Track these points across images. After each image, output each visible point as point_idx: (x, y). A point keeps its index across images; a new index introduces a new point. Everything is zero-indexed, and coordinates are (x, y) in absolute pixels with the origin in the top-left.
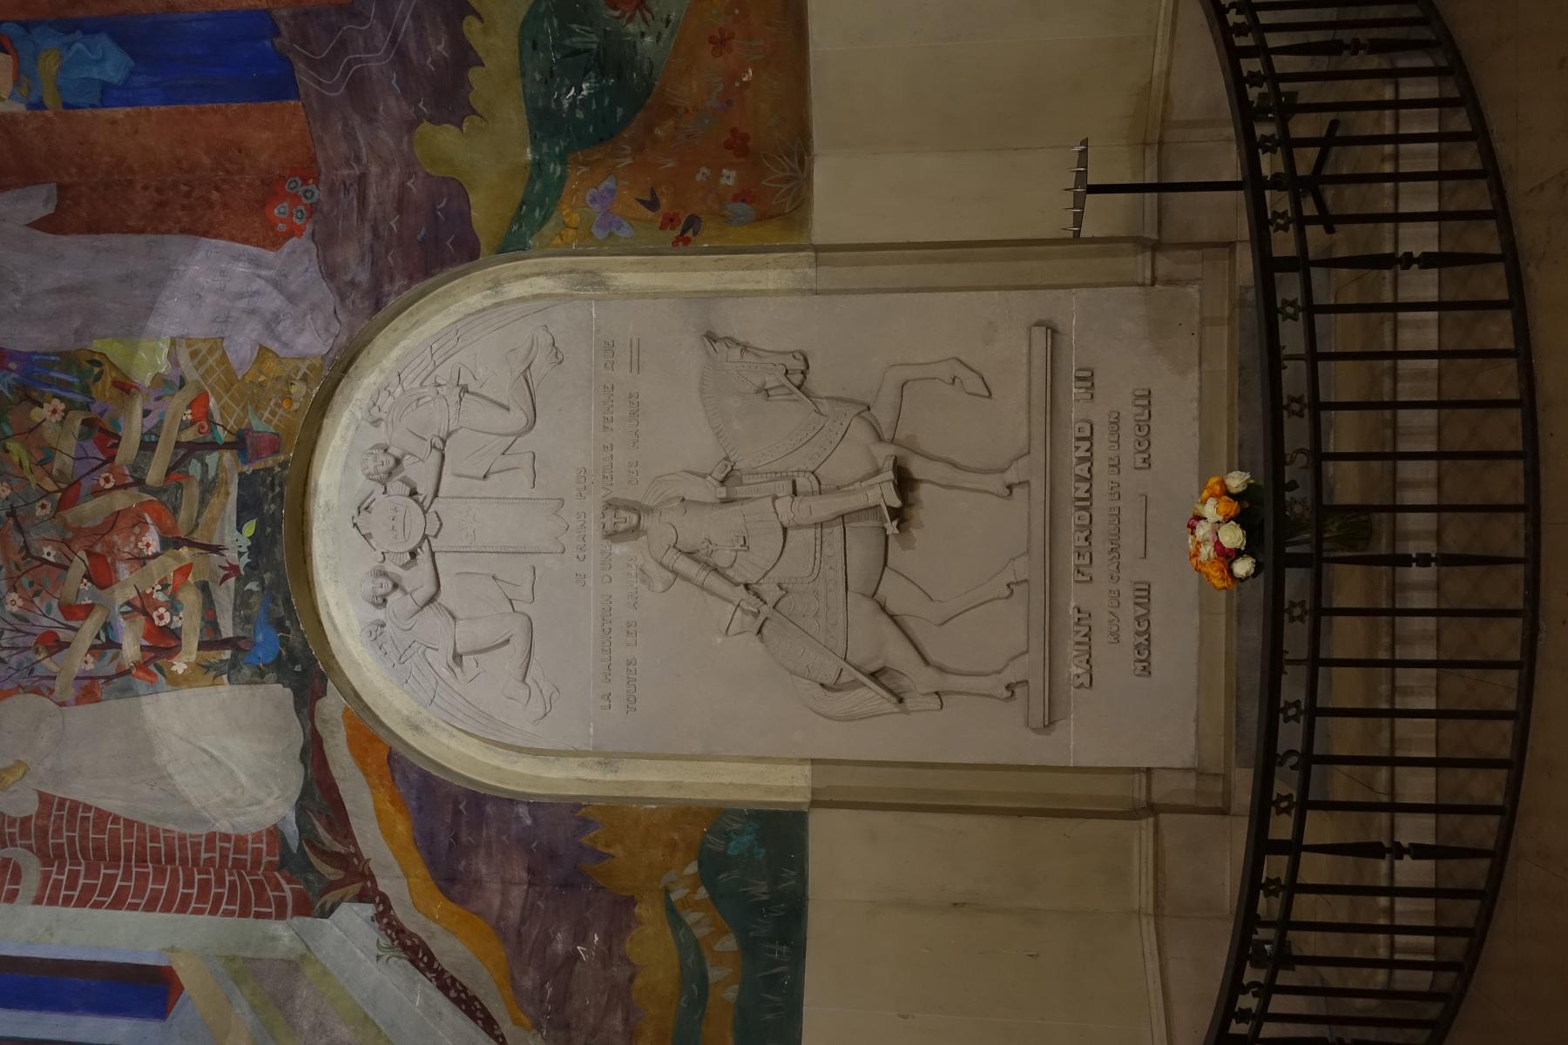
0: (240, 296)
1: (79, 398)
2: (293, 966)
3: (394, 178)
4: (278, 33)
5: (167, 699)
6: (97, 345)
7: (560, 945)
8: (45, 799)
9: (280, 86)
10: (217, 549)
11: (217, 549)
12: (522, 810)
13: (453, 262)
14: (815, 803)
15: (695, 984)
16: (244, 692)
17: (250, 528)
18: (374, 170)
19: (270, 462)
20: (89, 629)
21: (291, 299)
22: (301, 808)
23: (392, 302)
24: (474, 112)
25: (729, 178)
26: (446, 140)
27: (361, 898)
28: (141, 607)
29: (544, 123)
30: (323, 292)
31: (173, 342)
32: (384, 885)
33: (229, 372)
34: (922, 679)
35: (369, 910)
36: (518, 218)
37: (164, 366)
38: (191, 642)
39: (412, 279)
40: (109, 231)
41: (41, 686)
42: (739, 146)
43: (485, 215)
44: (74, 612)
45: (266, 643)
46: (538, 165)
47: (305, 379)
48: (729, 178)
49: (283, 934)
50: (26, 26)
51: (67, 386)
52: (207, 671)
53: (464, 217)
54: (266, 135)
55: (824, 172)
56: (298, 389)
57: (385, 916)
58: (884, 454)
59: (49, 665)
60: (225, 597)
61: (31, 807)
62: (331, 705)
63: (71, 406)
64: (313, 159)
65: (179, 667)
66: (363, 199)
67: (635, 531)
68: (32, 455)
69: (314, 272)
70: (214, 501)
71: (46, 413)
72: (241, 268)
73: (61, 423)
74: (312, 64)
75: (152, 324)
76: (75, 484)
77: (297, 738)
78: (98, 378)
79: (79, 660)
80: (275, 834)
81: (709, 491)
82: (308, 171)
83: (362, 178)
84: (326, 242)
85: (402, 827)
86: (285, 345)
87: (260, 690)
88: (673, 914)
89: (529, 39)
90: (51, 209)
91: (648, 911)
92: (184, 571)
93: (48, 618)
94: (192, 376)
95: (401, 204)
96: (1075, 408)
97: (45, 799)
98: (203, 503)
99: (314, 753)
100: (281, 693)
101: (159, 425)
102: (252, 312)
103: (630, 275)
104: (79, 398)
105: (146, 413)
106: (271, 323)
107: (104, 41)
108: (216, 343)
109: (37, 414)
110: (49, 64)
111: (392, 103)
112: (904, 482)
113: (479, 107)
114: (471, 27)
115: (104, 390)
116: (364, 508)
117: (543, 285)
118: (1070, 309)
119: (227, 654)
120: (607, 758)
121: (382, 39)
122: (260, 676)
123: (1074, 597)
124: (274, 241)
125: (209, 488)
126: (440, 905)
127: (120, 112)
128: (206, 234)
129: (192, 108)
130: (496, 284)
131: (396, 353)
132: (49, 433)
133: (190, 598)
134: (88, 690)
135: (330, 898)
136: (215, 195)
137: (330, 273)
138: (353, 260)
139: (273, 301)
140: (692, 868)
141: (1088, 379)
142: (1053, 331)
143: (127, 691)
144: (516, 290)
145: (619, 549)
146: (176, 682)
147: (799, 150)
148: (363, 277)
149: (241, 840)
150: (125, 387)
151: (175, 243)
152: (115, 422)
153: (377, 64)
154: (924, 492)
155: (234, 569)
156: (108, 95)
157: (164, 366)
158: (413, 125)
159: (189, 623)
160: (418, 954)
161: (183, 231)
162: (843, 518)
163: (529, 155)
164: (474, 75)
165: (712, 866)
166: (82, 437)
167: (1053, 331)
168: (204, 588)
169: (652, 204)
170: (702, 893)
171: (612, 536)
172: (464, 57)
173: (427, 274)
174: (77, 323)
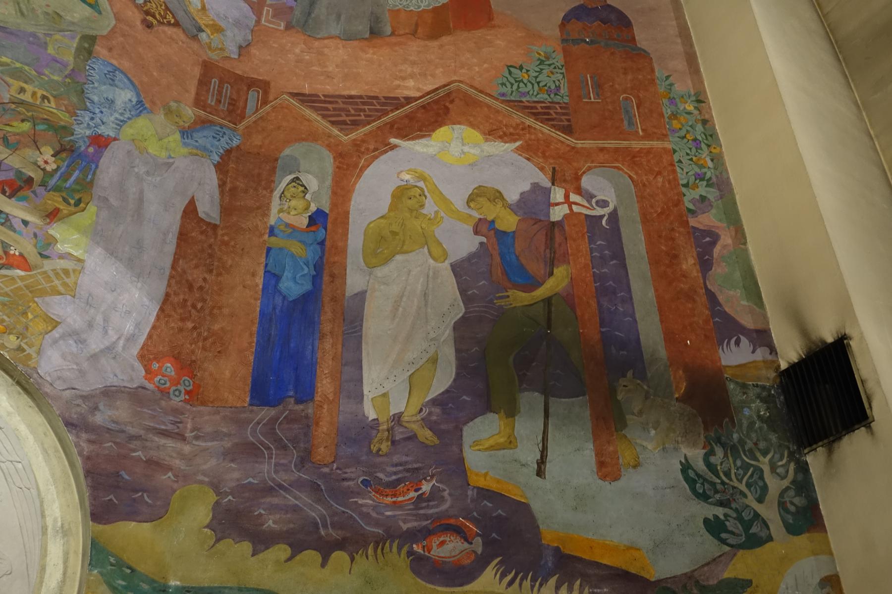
0: (106, 320)
1: (52, 182)
3: (177, 463)
4: (299, 401)
6: (92, 208)
13: (94, 498)
18: (187, 449)
21: (94, 357)
23: (70, 438)
24: (218, 540)
30: (93, 383)
31: (79, 260)
33: (43, 293)
36: (120, 564)
37: (61, 247)
39: (87, 459)
40: (178, 246)
47: (20, 349)
50: (322, 243)
51: (66, 176)
53: (132, 515)
54: (227, 373)
56: (12, 341)
64: (203, 403)
66: (165, 434)
68: (14, 135)
69: (112, 381)
71: (46, 156)
72: (129, 327)
73: (35, 164)
74: (273, 420)
75: (99, 250)
78: (65, 200)
82: (194, 396)
83: (182, 437)
84: (137, 396)
86: (55, 342)
90: (201, 215)
94: (48, 265)
95: (154, 464)
101: (12, 228)
102: (90, 325)
104: (52, 182)
105: (25, 223)
106: (76, 335)
107: (308, 286)
108: (72, 291)
109: (47, 152)
110: (296, 248)
111: (236, 475)
113: (221, 546)
114: (281, 551)
115: (55, 201)
121: (283, 478)
124: (143, 357)
127: (260, 281)
128: (162, 309)
129: (255, 328)
130: (65, 532)
131: (23, 429)
132: (30, 153)
136: (190, 325)
137: (109, 393)
139: (96, 343)
144: (55, 550)
148: (98, 419)
150: (53, 215)
151: (161, 288)
152: (25, 199)
156: (273, 277)
157: (61, 247)
158: (216, 487)
161: (167, 295)
163: (174, 583)
164: (246, 547)
166: (19, 173)
173: (88, 473)
174: (113, 201)
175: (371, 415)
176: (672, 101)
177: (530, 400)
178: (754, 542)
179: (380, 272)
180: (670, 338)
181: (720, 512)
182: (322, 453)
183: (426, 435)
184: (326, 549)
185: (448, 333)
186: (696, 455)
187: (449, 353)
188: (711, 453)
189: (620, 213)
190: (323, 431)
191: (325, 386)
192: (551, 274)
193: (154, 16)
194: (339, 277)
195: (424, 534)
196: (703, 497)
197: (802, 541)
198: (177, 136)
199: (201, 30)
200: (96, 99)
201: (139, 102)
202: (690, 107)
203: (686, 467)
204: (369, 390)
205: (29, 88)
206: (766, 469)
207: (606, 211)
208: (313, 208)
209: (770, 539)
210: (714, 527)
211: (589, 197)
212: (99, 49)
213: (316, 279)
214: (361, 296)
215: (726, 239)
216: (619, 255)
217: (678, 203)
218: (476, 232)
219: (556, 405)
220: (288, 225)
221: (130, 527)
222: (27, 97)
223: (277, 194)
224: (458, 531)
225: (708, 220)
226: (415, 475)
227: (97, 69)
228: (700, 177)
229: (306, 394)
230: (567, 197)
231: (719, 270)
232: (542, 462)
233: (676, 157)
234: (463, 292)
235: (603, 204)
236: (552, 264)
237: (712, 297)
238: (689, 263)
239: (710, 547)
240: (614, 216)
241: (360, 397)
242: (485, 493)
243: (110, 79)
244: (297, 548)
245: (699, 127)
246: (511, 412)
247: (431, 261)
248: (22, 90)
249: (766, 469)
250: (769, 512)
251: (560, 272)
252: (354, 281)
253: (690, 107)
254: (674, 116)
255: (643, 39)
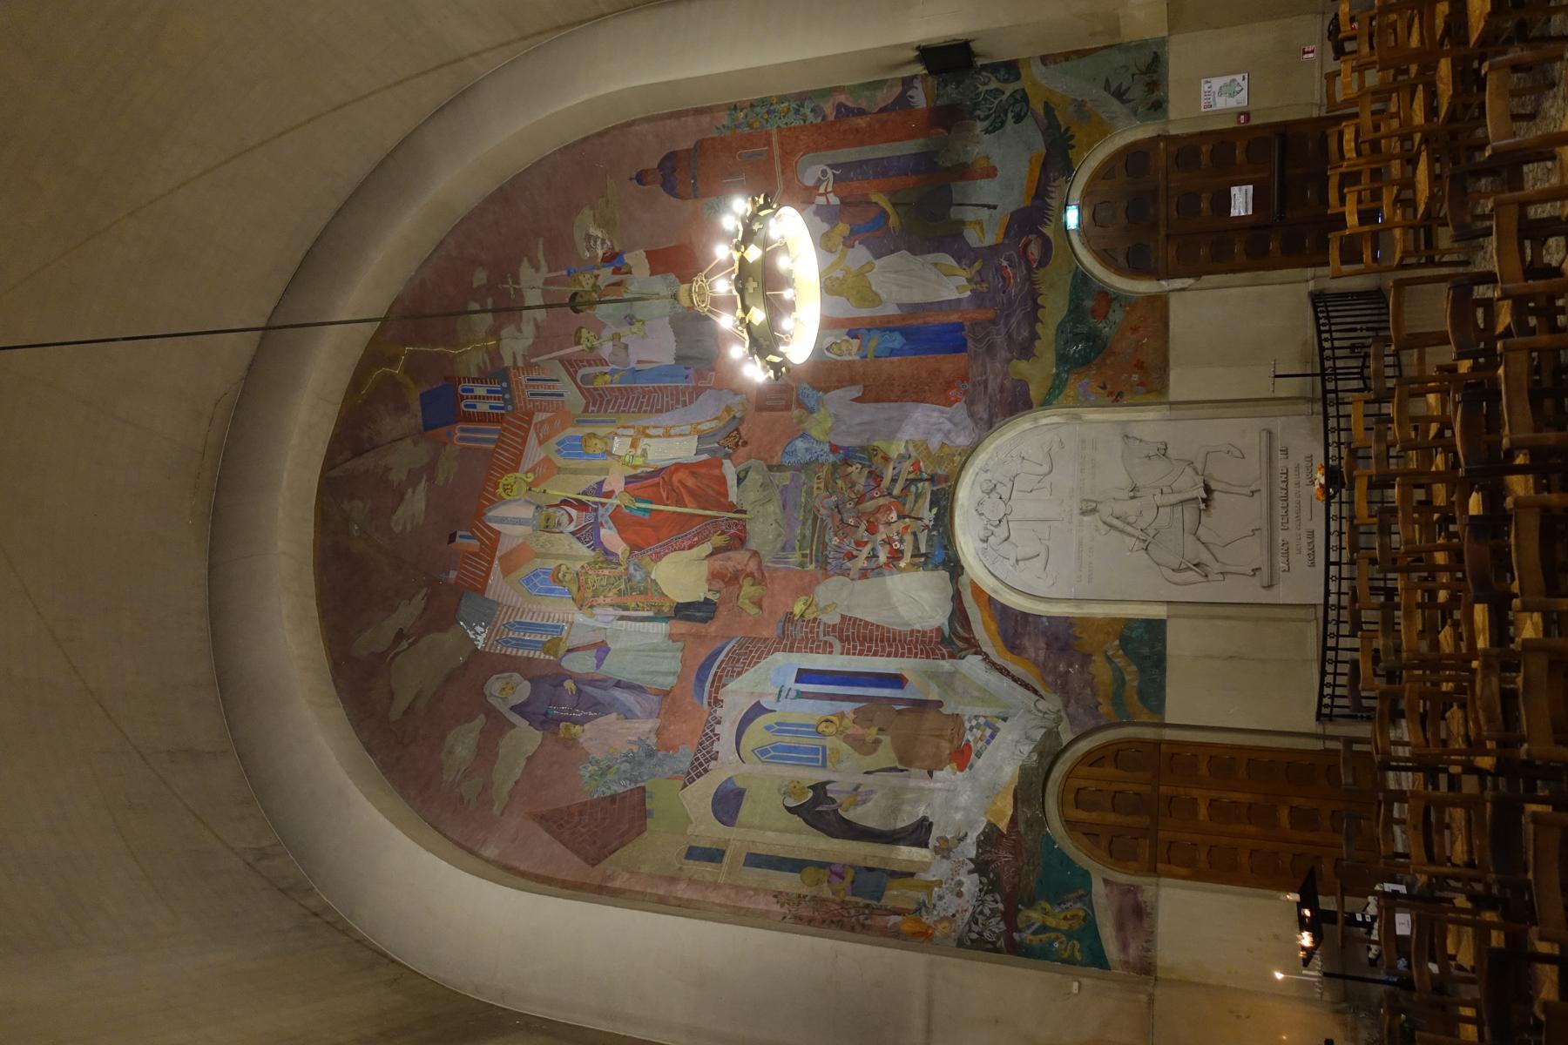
0: (935, 424)
1: (867, 463)
2: (952, 674)
3: (999, 380)
4: (964, 330)
5: (897, 577)
6: (875, 444)
7: (1062, 668)
8: (843, 617)
9: (960, 347)
10: (921, 519)
11: (921, 519)
12: (1045, 619)
13: (1023, 410)
14: (1168, 617)
15: (1120, 681)
16: (929, 574)
17: (935, 511)
18: (991, 377)
19: (944, 485)
20: (866, 550)
21: (955, 425)
22: (951, 620)
23: (997, 425)
24: (1034, 355)
25: (1135, 377)
26: (1022, 366)
27: (976, 653)
28: (888, 542)
29: (1062, 359)
30: (969, 422)
31: (907, 442)
32: (984, 649)
33: (929, 453)
34: (1216, 567)
35: (980, 657)
36: (1049, 394)
37: (902, 450)
38: (908, 555)
39: (1005, 417)
40: (883, 401)
41: (845, 573)
42: (1140, 366)
43: (1035, 392)
44: (860, 544)
45: (939, 555)
46: (1058, 375)
47: (960, 454)
48: (1135, 377)
49: (946, 665)
50: (869, 330)
51: (863, 459)
52: (914, 566)
54: (951, 366)
55: (1173, 375)
56: (957, 458)
57: (986, 658)
58: (1199, 479)
59: (849, 564)
60: (923, 537)
61: (837, 620)
62: (963, 579)
63: (863, 466)
64: (967, 374)
65: (902, 564)
66: (986, 387)
67: (1094, 511)
70: (920, 502)
71: (854, 469)
72: (936, 414)
73: (860, 473)
74: (974, 340)
75: (899, 435)
76: (864, 495)
77: (951, 592)
79: (861, 562)
80: (939, 630)
81: (1126, 494)
82: (964, 378)
83: (986, 381)
84: (970, 404)
85: (993, 627)
86: (952, 442)
87: (936, 573)
88: (1109, 659)
89: (1060, 329)
90: (860, 394)
91: (1098, 659)
92: (907, 528)
93: (849, 546)
94: (914, 454)
95: (1002, 389)
96: (1280, 463)
97: (843, 617)
98: (916, 502)
99: (957, 598)
100: (946, 575)
101: (900, 472)
102: (940, 430)
103: (1092, 415)
104: (867, 463)
105: (894, 468)
106: (947, 434)
107: (897, 335)
108: (924, 442)
109: (850, 469)
110: (873, 343)
111: (1003, 353)
112: (1208, 490)
113: (1037, 354)
114: (1039, 327)
115: (877, 460)
116: (980, 503)
117: (1055, 419)
118: (1278, 424)
119: (923, 559)
120: (1078, 601)
121: (1003, 331)
122: (936, 567)
123: (1281, 536)
124: (950, 405)
125: (918, 496)
126: (1009, 655)
127: (896, 359)
128: (922, 402)
129: (923, 357)
130: (1036, 419)
131: (993, 446)
132: (854, 477)
133: (909, 538)
134: (864, 574)
135: (963, 653)
136: (927, 388)
137: (972, 415)
138: (981, 411)
139: (948, 426)
140: (1117, 642)
141: (1285, 451)
142: (1270, 433)
143: (881, 574)
144: (1044, 421)
145: (1086, 519)
146: (901, 570)
147: (1164, 367)
148: (985, 416)
149: (924, 633)
150: (886, 459)
151: (909, 405)
152: (881, 471)
153: (1000, 340)
154: (1216, 495)
155: (927, 526)
156: (893, 352)
157: (902, 450)
158: (1009, 361)
159: (908, 548)
160: (1003, 671)
161: (913, 401)
162: (1182, 502)
164: (1037, 343)
165: (1125, 642)
166: (868, 478)
167: (1270, 433)
168: (914, 534)
169: (1104, 388)
170: (1121, 652)
171: (1084, 513)
172: (1034, 336)
173: (1011, 415)
174: (867, 436)
175: (969, 293)
176: (737, 127)
177: (954, 213)
178: (1025, 98)
179: (884, 297)
180: (911, 136)
181: (1010, 115)
182: (990, 314)
183: (977, 265)
184: (1037, 307)
185: (918, 258)
186: (980, 126)
187: (931, 257)
188: (978, 117)
189: (830, 162)
190: (979, 316)
191: (954, 318)
192: (876, 203)
193: (737, 443)
194: (889, 318)
195: (1028, 262)
196: (1003, 123)
197: (1023, 73)
198: (815, 415)
199: (734, 417)
200: (808, 457)
201: (801, 436)
202: (742, 115)
203: (987, 131)
204: (955, 295)
205: (815, 486)
206: (986, 88)
207: (830, 172)
208: (846, 338)
209: (1023, 90)
210: (1018, 119)
211: (820, 182)
212: (775, 462)
213: (892, 330)
214: (900, 306)
215: (842, 98)
216: (860, 164)
217: (818, 127)
218: (853, 247)
219: (956, 198)
220: (859, 349)
221: (1032, 393)
222: (822, 486)
223: (839, 358)
224: (1026, 246)
225: (829, 108)
226: (999, 269)
227: (787, 460)
228: (797, 112)
229: (959, 327)
230: (821, 195)
231: (864, 104)
232: (989, 207)
233: (783, 126)
234: (892, 252)
235: (824, 173)
236: (870, 203)
237: (881, 111)
238: (861, 122)
239: (1028, 121)
240: (832, 167)
241: (959, 300)
242: (1006, 234)
243: (794, 452)
244: (1037, 320)
245: (757, 109)
246: (962, 223)
247: (875, 270)
248: (818, 488)
249: (986, 88)
250: (1010, 88)
251: (874, 198)
252: (891, 310)
253: (742, 115)
254: (750, 126)
255: (684, 145)
